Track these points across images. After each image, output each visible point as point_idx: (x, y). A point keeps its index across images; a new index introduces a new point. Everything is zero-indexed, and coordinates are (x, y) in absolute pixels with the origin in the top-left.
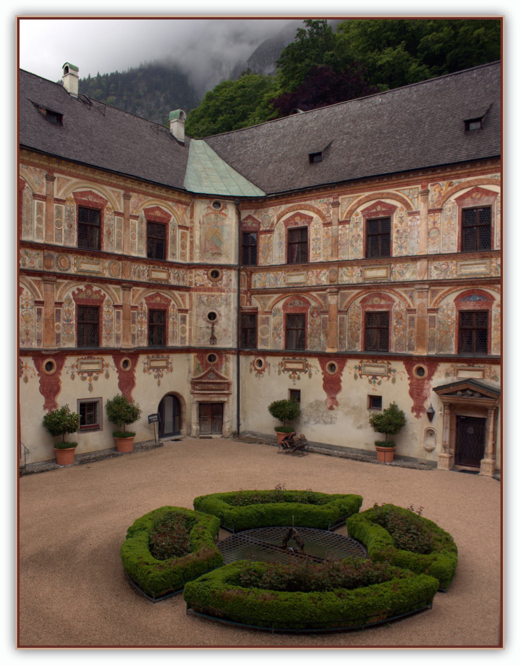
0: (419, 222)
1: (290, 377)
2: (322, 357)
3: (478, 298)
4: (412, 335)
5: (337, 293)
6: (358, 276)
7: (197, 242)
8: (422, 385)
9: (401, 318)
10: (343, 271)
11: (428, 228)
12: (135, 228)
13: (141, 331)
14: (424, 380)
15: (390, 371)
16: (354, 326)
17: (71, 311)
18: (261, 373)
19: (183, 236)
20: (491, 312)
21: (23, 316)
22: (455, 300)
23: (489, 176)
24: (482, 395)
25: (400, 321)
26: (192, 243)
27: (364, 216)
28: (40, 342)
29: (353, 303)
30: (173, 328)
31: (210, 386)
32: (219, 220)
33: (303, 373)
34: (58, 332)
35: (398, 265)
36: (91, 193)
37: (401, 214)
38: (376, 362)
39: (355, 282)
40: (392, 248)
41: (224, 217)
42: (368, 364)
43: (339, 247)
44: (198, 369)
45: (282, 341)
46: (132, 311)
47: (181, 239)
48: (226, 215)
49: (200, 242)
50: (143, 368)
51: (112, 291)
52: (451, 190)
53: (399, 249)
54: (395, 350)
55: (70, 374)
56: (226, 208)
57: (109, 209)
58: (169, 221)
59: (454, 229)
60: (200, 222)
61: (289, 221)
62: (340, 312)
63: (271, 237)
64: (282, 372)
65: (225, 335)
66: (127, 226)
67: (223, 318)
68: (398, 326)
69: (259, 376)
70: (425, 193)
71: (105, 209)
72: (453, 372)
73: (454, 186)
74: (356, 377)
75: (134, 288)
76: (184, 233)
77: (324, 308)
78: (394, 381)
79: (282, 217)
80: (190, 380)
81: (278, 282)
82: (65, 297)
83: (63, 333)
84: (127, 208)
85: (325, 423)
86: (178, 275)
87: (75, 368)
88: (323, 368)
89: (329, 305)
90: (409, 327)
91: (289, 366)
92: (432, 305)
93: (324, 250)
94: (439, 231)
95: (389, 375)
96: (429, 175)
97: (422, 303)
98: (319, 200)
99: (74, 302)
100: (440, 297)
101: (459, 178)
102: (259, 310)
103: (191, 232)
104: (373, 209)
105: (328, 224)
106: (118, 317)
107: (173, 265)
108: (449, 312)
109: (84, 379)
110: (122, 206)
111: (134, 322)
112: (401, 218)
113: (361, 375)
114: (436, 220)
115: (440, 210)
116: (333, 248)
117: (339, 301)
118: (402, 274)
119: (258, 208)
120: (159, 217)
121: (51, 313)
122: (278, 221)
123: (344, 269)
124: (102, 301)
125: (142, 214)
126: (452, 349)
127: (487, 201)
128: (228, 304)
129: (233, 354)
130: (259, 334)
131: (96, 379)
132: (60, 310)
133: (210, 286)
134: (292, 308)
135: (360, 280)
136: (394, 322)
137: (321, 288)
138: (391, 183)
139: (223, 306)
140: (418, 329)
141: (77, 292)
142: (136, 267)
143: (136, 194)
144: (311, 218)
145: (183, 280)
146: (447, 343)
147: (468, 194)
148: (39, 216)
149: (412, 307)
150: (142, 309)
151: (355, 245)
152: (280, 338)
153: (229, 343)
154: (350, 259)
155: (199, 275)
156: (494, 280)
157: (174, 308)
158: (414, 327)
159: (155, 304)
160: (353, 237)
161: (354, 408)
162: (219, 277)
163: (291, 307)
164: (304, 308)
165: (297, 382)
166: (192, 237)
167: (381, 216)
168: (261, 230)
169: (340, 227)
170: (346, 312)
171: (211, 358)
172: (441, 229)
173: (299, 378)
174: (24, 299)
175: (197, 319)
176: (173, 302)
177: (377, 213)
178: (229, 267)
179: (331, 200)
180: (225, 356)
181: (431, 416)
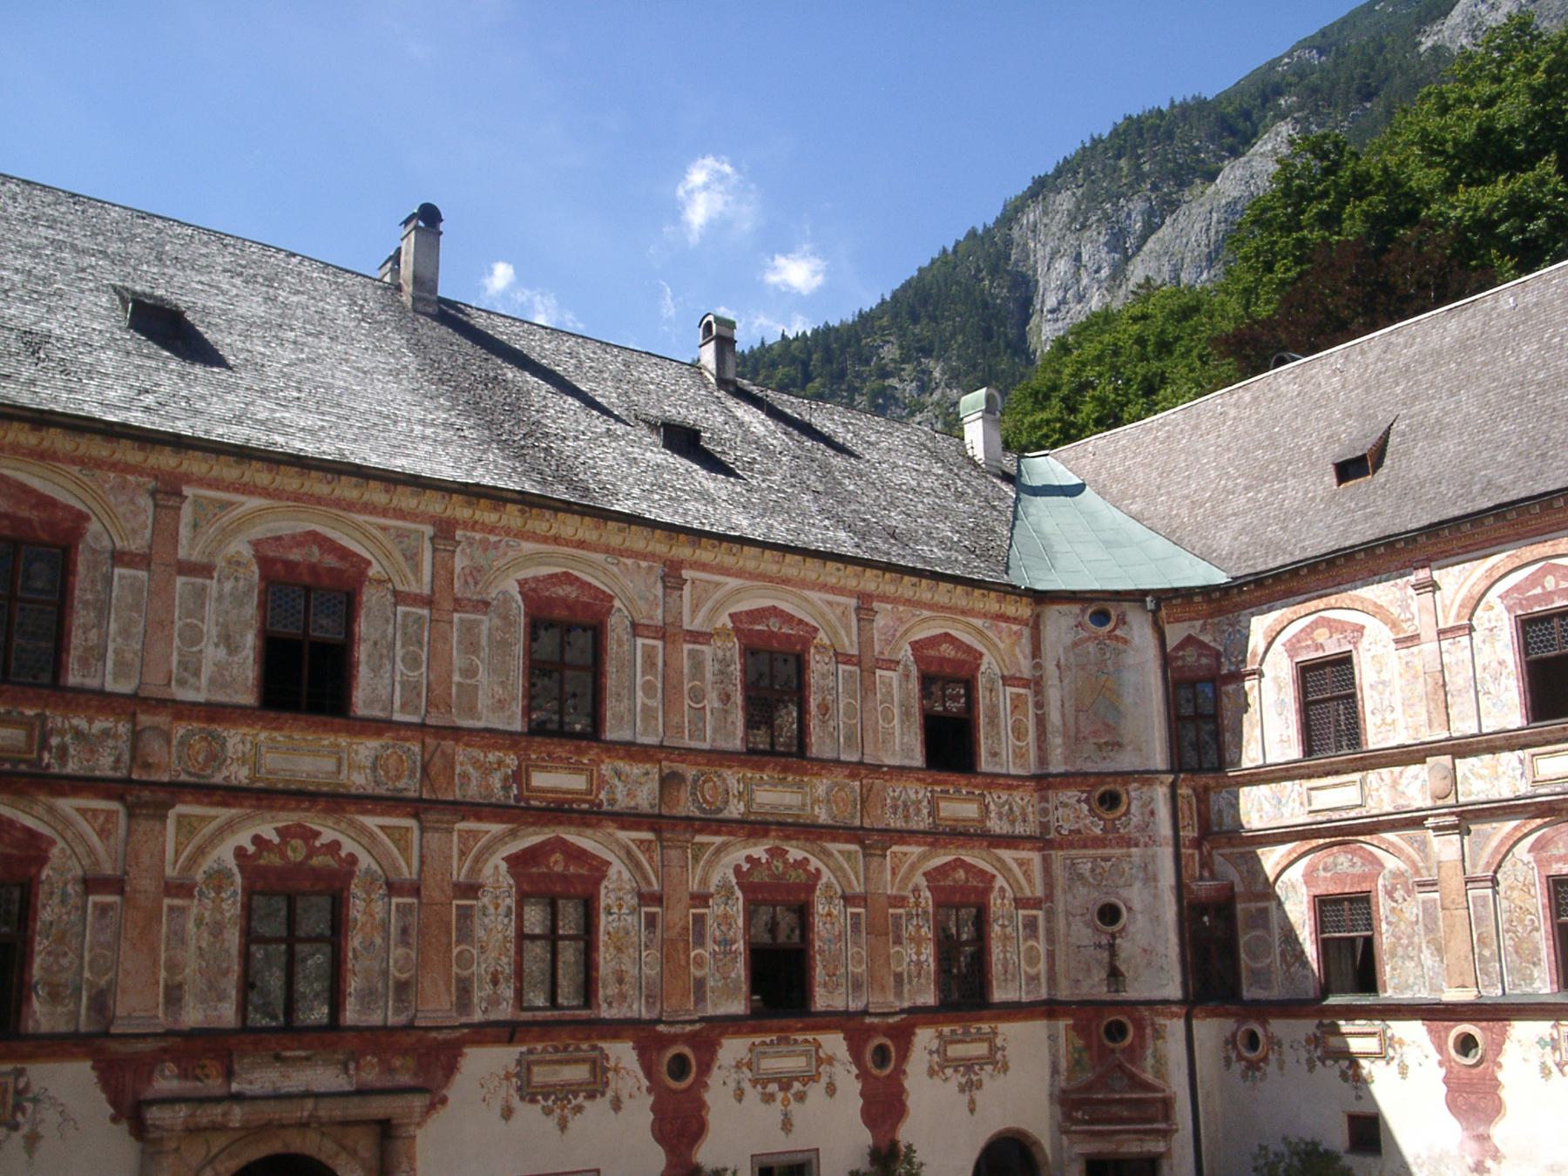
2: (1433, 1013)
6: (1514, 777)
7: (1054, 717)
12: (890, 693)
13: (919, 963)
16: (1521, 921)
17: (732, 916)
18: (1259, 1069)
19: (1017, 703)
21: (609, 933)
26: (1041, 721)
27: (1509, 609)
28: (654, 1003)
30: (1005, 952)
31: (1115, 1109)
32: (1108, 655)
33: (1381, 1063)
34: (699, 974)
36: (774, 611)
39: (1507, 794)
41: (1121, 646)
44: (1078, 1062)
46: (891, 911)
47: (1012, 712)
48: (1126, 642)
49: (1063, 715)
50: (926, 1066)
51: (836, 859)
55: (732, 1085)
56: (1125, 623)
57: (821, 649)
58: (978, 666)
60: (1058, 666)
61: (1299, 641)
64: (1319, 1064)
65: (1149, 964)
66: (868, 688)
67: (1139, 916)
69: (1254, 1077)
71: (812, 651)
74: (1545, 1072)
75: (895, 848)
76: (1019, 695)
77: (1424, 872)
79: (1279, 633)
80: (1057, 1092)
81: (1284, 810)
82: (715, 879)
83: (713, 975)
84: (865, 641)
86: (1011, 809)
87: (745, 1069)
88: (1440, 1048)
89: (1439, 864)
99: (739, 894)
102: (1236, 889)
103: (1037, 694)
104: (1534, 588)
105: (1408, 641)
106: (856, 927)
107: (995, 781)
109: (769, 1098)
110: (855, 638)
111: (898, 941)
116: (1432, 705)
119: (1211, 616)
120: (949, 660)
121: (681, 924)
122: (1270, 645)
124: (811, 889)
125: (906, 653)
128: (1151, 879)
129: (1174, 1015)
130: (1243, 956)
131: (801, 1097)
132: (703, 916)
133: (1098, 831)
134: (1332, 879)
135: (1524, 788)
139: (1138, 885)
141: (746, 866)
142: (896, 794)
143: (889, 607)
144: (1361, 629)
145: (1024, 821)
148: (648, 678)
150: (917, 905)
151: (1492, 690)
153: (1162, 986)
155: (1065, 805)
157: (1003, 898)
159: (953, 889)
162: (1123, 808)
163: (1329, 875)
164: (1364, 877)
166: (1039, 705)
168: (1224, 672)
169: (1445, 644)
171: (1116, 1031)
174: (614, 890)
175: (1069, 925)
176: (1000, 881)
177: (1548, 595)
178: (1146, 777)
180: (1153, 1024)
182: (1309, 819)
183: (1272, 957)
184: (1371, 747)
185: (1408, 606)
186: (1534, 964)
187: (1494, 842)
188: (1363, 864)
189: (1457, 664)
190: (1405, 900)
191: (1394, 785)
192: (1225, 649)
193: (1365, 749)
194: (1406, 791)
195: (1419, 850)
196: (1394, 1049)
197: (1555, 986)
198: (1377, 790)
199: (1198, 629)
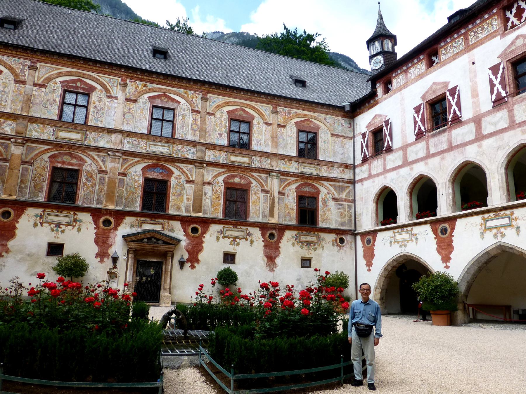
0: (116, 105)
3: (161, 171)
4: (101, 192)
6: (50, 135)
9: (91, 177)
10: (31, 126)
11: (124, 111)
14: (111, 230)
15: (75, 221)
16: (39, 178)
20: (171, 182)
23: (175, 89)
24: (165, 243)
25: (90, 179)
27: (62, 86)
29: (41, 157)
35: (93, 133)
38: (61, 212)
39: (45, 138)
42: (52, 213)
43: (31, 105)
53: (95, 121)
54: (82, 203)
59: (145, 117)
62: (24, 162)
68: (87, 183)
70: (124, 85)
72: (137, 224)
73: (148, 88)
74: (35, 225)
78: (79, 230)
90: (99, 185)
93: (11, 103)
95: (74, 224)
97: (114, 167)
98: (14, 59)
100: (130, 165)
101: (152, 83)
108: (137, 178)
112: (100, 98)
113: (41, 224)
114: (131, 107)
115: (135, 101)
116: (24, 105)
117: (25, 152)
123: (35, 125)
126: (137, 206)
135: (52, 138)
140: (108, 188)
146: (133, 202)
147: (158, 97)
149: (104, 169)
151: (49, 107)
158: (104, 186)
169: (35, 88)
170: (31, 164)
172: (135, 115)
179: (29, 63)
181: (115, 260)
185: (24, 72)
186: (40, 192)
189: (38, 95)
195: (4, 148)
197: (46, 200)
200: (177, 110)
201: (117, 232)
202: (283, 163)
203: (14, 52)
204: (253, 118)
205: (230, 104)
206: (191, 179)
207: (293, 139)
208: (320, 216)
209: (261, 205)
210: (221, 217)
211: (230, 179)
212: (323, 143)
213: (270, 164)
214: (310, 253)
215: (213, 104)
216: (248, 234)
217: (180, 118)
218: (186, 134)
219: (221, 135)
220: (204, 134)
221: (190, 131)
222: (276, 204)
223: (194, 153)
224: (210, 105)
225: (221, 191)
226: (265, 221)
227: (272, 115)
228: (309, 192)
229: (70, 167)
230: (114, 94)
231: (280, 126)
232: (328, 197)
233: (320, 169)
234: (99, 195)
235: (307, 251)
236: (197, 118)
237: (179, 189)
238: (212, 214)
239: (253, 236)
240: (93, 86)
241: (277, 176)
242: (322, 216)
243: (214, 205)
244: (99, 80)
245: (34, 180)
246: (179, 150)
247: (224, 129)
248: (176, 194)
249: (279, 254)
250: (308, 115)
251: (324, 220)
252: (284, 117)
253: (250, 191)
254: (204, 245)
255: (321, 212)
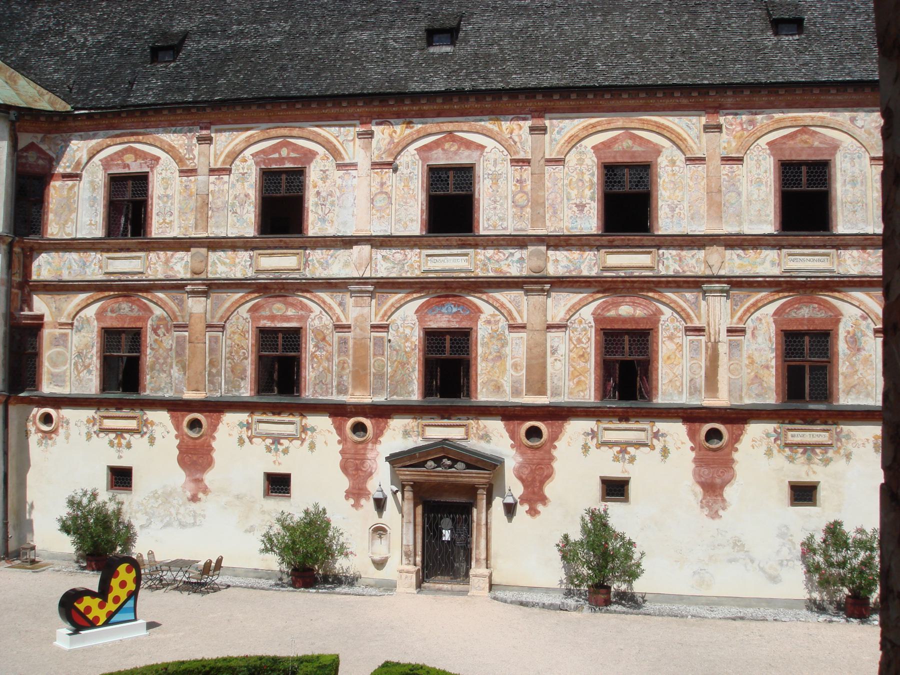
1: (111, 444)
2: (175, 406)
3: (455, 310)
4: (343, 368)
5: (205, 294)
6: (245, 266)
8: (362, 452)
9: (324, 339)
10: (213, 256)
15: (304, 429)
16: (237, 353)
18: (51, 439)
22: (416, 312)
25: (321, 344)
27: (257, 164)
33: (138, 436)
37: (325, 166)
39: (239, 275)
40: (307, 220)
43: (210, 213)
45: (94, 378)
52: (409, 135)
62: (209, 326)
63: (73, 186)
64: (94, 436)
68: (318, 353)
69: (47, 444)
72: (415, 429)
74: (241, 441)
77: (180, 319)
78: (312, 447)
79: (98, 152)
81: (87, 270)
85: (182, 525)
88: (178, 427)
89: (191, 315)
90: (339, 356)
91: (108, 424)
92: (378, 318)
93: (179, 216)
94: (390, 198)
95: (303, 436)
96: (375, 106)
97: (362, 316)
102: (46, 319)
104: (275, 153)
108: (408, 331)
112: (324, 172)
113: (250, 438)
116: (199, 215)
117: (209, 307)
118: (325, 265)
122: (90, 159)
126: (413, 391)
127: (469, 156)
135: (250, 273)
136: (309, 346)
137: (175, 286)
138: (308, 112)
140: (355, 359)
144: (157, 159)
147: (437, 144)
149: (344, 322)
151: (238, 211)
152: (90, 372)
154: (230, 235)
156: (482, 282)
158: (348, 356)
160: (236, 197)
161: (238, 497)
163: (114, 315)
164: (139, 319)
165: (125, 452)
167: (288, 165)
169: (212, 178)
173: (129, 446)
177: (282, 160)
182: (105, 278)
183: (68, 366)
184: (153, 236)
185: (192, 150)
186: (242, 379)
187: (227, 305)
188: (139, 310)
189: (219, 191)
190: (165, 335)
191: (167, 262)
192: (57, 157)
193: (149, 237)
194: (174, 267)
196: (147, 428)
197: (253, 393)
198: (155, 264)
199: (39, 140)
200: (479, 165)
201: (379, 447)
202: (738, 255)
203: (172, 118)
204: (658, 151)
205: (599, 128)
206: (519, 321)
207: (763, 188)
208: (841, 378)
209: (686, 363)
210: (592, 400)
211: (609, 310)
212: (848, 187)
213: (706, 262)
214: (814, 472)
215: (558, 137)
216: (656, 435)
217: (488, 182)
218: (501, 219)
219: (581, 207)
220: (541, 211)
221: (511, 211)
222: (723, 360)
223: (521, 259)
224: (551, 140)
225: (589, 339)
226: (695, 402)
227: (705, 137)
228: (811, 320)
229: (285, 325)
230: (349, 158)
231: (727, 160)
232: (863, 327)
233: (839, 256)
234: (340, 376)
235: (806, 468)
236: (524, 176)
237: (495, 345)
238: (571, 393)
239: (667, 438)
240: (310, 151)
241: (722, 291)
242: (845, 377)
243: (576, 375)
244: (320, 135)
245: (230, 357)
246: (489, 259)
247: (588, 193)
248: (490, 357)
249: (733, 476)
250: (802, 119)
251: (854, 387)
252: (739, 134)
253: (657, 332)
254: (555, 465)
255: (843, 367)
